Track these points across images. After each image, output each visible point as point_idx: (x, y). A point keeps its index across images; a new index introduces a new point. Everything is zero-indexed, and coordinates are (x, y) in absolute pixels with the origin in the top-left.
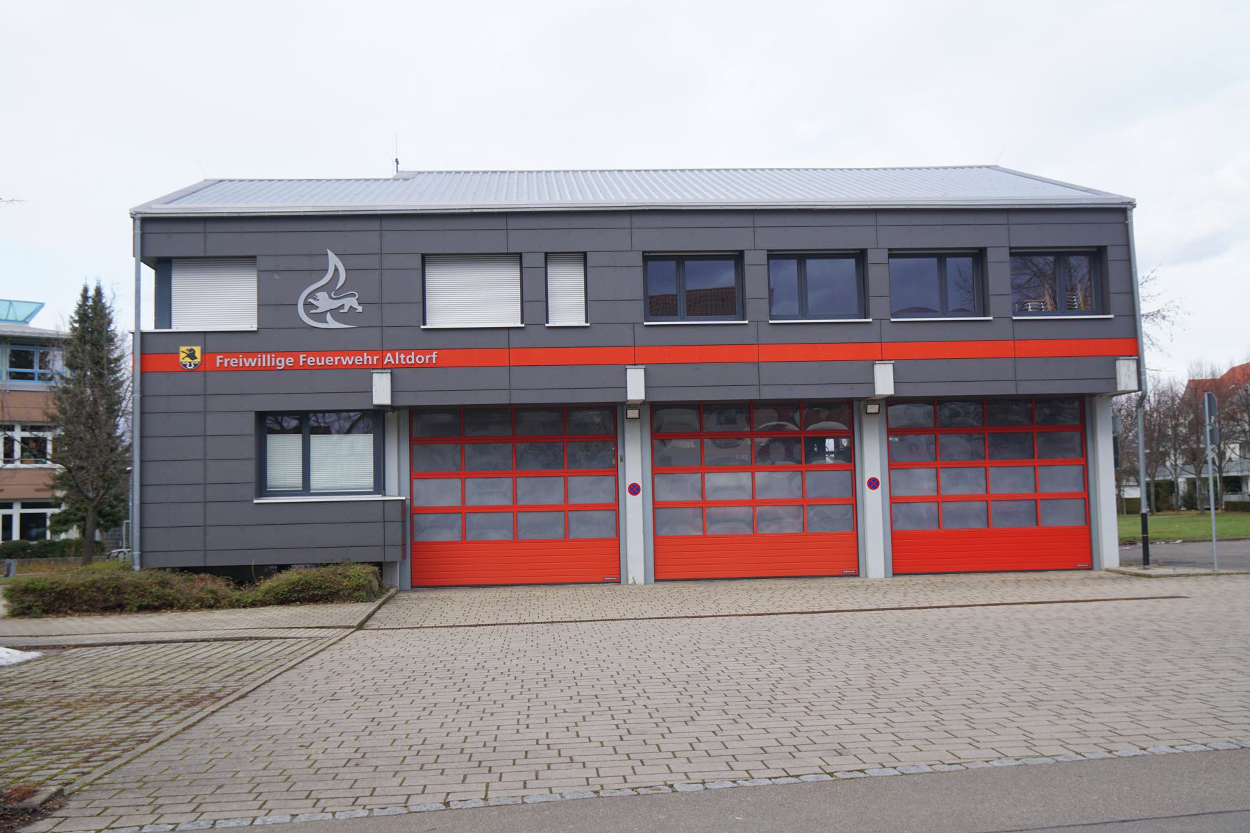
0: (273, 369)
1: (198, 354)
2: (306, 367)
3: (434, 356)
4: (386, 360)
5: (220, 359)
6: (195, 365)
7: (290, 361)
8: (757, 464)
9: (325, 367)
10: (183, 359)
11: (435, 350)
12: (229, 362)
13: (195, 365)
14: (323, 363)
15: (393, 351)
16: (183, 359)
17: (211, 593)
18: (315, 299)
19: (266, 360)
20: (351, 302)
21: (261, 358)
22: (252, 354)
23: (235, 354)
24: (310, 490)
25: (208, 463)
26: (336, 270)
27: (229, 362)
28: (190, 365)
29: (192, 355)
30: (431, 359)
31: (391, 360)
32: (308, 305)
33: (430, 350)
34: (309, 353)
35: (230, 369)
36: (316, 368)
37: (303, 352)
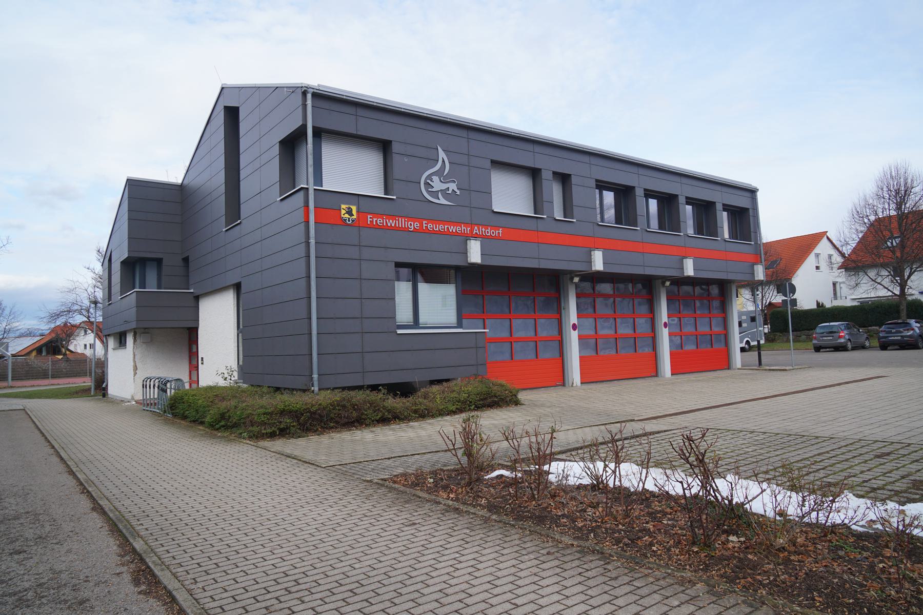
0: (406, 230)
1: (354, 212)
2: (428, 231)
3: (500, 232)
4: (475, 232)
5: (370, 218)
6: (353, 221)
7: (417, 225)
8: (684, 313)
9: (439, 232)
10: (344, 215)
11: (501, 227)
12: (376, 221)
13: (353, 221)
14: (437, 229)
15: (478, 225)
16: (344, 215)
17: (235, 423)
18: (431, 181)
19: (402, 223)
20: (453, 186)
21: (398, 220)
22: (393, 217)
23: (380, 215)
24: (419, 324)
25: (363, 301)
26: (443, 161)
27: (376, 221)
28: (349, 221)
29: (350, 212)
30: (499, 233)
31: (477, 232)
32: (427, 184)
33: (497, 228)
34: (430, 221)
35: (377, 227)
36: (434, 232)
37: (425, 220)
